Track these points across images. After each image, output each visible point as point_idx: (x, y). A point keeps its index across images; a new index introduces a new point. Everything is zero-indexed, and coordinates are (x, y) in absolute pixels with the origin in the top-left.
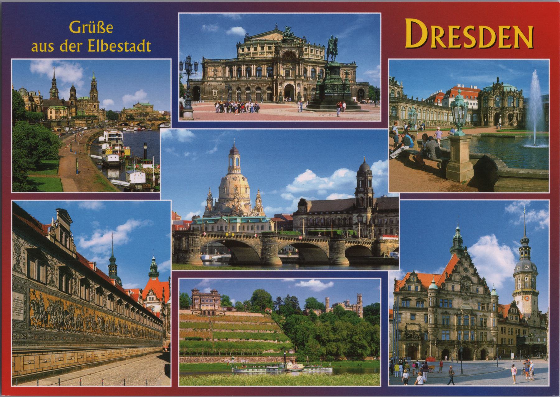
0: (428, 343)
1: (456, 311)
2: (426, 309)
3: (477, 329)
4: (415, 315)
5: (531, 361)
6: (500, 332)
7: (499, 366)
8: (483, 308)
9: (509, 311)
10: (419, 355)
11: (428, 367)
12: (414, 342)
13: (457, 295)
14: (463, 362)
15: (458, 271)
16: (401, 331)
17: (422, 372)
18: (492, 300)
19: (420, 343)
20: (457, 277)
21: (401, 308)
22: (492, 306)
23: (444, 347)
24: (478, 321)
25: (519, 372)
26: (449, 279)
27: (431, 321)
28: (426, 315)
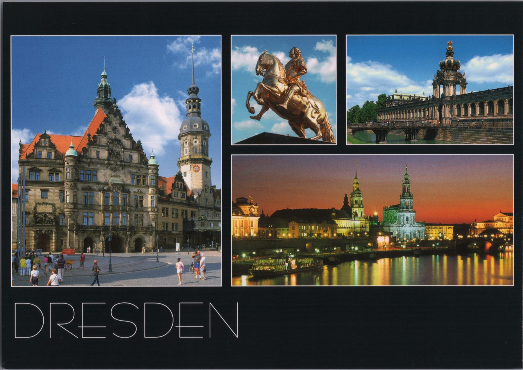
0: (64, 229)
1: (102, 186)
2: (62, 184)
3: (131, 210)
4: (47, 191)
5: (202, 254)
6: (161, 214)
7: (160, 260)
8: (138, 181)
9: (173, 185)
10: (53, 246)
11: (65, 262)
12: (46, 228)
13: (102, 164)
14: (113, 255)
15: (104, 131)
16: (28, 213)
17: (57, 268)
18: (150, 171)
19: (54, 229)
20: (104, 140)
21: (28, 182)
22: (149, 180)
23: (86, 235)
24: (132, 199)
25: (186, 269)
26: (93, 142)
27: (68, 200)
28: (62, 191)
